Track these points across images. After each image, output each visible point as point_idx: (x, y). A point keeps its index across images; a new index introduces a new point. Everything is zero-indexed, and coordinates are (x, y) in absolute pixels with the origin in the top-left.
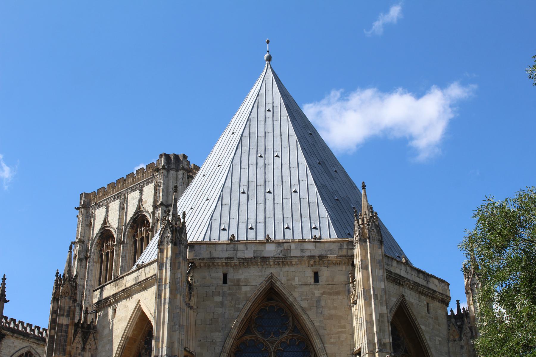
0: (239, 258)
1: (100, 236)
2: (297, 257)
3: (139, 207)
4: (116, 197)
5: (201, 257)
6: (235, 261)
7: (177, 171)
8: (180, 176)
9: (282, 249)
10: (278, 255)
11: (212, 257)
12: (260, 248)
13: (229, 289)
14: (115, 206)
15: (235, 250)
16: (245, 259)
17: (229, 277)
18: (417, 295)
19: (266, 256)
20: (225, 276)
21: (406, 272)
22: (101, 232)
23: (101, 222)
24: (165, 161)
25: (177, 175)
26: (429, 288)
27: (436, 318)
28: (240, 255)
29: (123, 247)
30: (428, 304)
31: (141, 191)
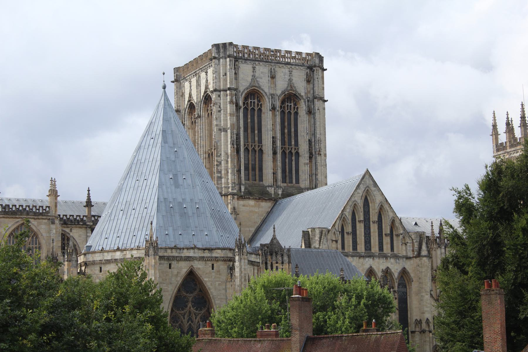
0: (105, 260)
1: (189, 107)
2: (129, 258)
3: (207, 87)
4: (194, 74)
5: (89, 260)
6: (104, 261)
7: (226, 58)
8: (228, 63)
9: (123, 254)
10: (121, 258)
11: (94, 260)
12: (114, 254)
13: (102, 275)
14: (194, 80)
15: (103, 256)
16: (107, 260)
17: (102, 269)
18: (204, 262)
19: (116, 258)
20: (101, 268)
21: (194, 253)
22: (189, 103)
23: (188, 95)
24: (216, 51)
25: (226, 62)
26: (212, 257)
27: (219, 271)
28: (106, 258)
29: (200, 120)
30: (213, 265)
31: (207, 73)
